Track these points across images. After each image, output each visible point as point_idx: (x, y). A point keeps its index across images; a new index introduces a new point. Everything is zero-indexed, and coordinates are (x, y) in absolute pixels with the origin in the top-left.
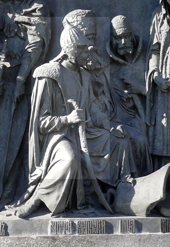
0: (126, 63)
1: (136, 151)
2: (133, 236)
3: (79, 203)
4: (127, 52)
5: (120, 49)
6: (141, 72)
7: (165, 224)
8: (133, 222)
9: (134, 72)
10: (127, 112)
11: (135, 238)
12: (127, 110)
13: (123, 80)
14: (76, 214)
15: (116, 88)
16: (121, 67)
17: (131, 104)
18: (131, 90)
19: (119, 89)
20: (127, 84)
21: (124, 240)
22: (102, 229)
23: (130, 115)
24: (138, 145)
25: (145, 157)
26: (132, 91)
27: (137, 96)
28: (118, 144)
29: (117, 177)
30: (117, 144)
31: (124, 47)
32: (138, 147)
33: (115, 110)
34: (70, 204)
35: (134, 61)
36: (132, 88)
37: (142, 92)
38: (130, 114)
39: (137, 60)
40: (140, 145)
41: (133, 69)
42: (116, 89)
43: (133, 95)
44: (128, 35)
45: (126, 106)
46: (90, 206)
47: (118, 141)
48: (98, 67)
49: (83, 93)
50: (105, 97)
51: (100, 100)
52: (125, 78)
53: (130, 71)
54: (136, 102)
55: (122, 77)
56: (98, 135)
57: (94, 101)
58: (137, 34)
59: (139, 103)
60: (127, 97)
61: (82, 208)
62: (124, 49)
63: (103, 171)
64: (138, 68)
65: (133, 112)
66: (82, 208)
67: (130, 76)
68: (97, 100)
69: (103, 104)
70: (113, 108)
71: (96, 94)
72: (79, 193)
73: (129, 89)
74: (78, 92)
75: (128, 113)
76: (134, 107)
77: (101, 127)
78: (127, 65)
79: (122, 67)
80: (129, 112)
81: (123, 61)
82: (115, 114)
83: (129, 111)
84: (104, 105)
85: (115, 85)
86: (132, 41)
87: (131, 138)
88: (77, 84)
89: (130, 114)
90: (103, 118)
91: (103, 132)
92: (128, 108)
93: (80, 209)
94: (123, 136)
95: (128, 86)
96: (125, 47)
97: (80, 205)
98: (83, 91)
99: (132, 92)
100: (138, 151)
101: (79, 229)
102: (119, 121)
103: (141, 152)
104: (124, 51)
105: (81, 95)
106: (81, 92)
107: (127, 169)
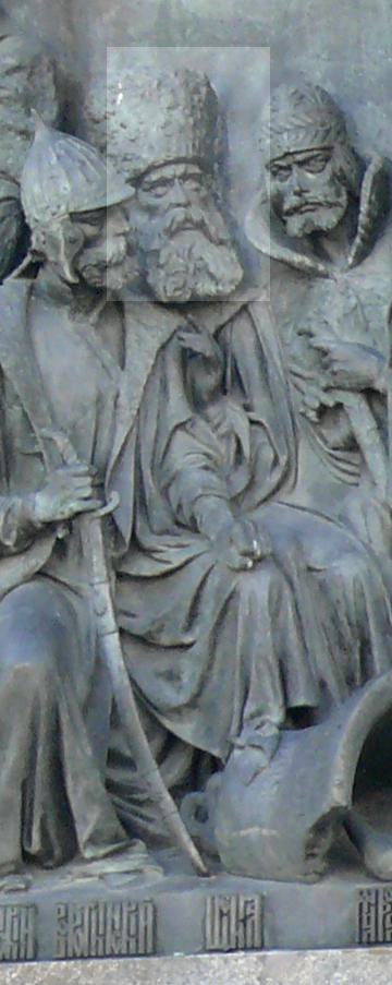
0: (321, 267)
1: (335, 620)
2: (240, 962)
3: (83, 833)
4: (312, 222)
5: (289, 213)
6: (380, 302)
7: (373, 909)
8: (253, 908)
9: (353, 301)
10: (334, 461)
11: (245, 969)
12: (331, 455)
13: (311, 335)
14: (70, 877)
15: (298, 369)
16: (311, 287)
17: (336, 435)
18: (334, 373)
19: (306, 374)
20: (325, 353)
21: (205, 979)
22: (141, 937)
23: (343, 476)
24: (336, 593)
25: (365, 646)
26: (337, 378)
27: (360, 396)
28: (233, 595)
29: (234, 728)
30: (231, 597)
31: (301, 206)
32: (338, 602)
33: (283, 459)
34: (52, 832)
35: (350, 260)
36: (336, 367)
37: (372, 381)
38: (344, 471)
39: (362, 256)
40: (345, 596)
41: (351, 292)
42: (296, 375)
43: (341, 397)
44: (312, 158)
45: (326, 442)
46: (141, 845)
47: (233, 585)
48: (206, 288)
49: (123, 400)
50: (239, 408)
51: (216, 422)
52: (314, 328)
53: (338, 300)
54: (354, 424)
55: (304, 326)
56: (176, 563)
57: (181, 426)
58: (366, 151)
59: (369, 427)
60: (317, 405)
61: (102, 851)
62: (302, 213)
63: (193, 704)
64: (367, 284)
65: (353, 464)
66: (102, 851)
67: (339, 321)
68: (201, 423)
69: (225, 436)
70: (275, 451)
71: (197, 402)
72: (80, 794)
73: (328, 372)
74: (100, 400)
75: (337, 467)
76: (352, 445)
77: (193, 527)
78: (326, 276)
79: (313, 284)
80: (340, 465)
81: (308, 261)
82: (285, 476)
83: (337, 459)
84: (233, 440)
85: (294, 359)
86: (339, 178)
87: (310, 569)
88: (98, 362)
89: (344, 471)
90: (200, 492)
91: (196, 546)
92: (334, 449)
93: (94, 859)
94: (250, 564)
95: (325, 360)
96: (308, 207)
97: (92, 841)
98: (122, 392)
99: (335, 382)
100: (344, 619)
101: (59, 938)
102: (303, 503)
103: (350, 624)
104: (305, 225)
105: (116, 405)
106: (118, 396)
107: (272, 696)
